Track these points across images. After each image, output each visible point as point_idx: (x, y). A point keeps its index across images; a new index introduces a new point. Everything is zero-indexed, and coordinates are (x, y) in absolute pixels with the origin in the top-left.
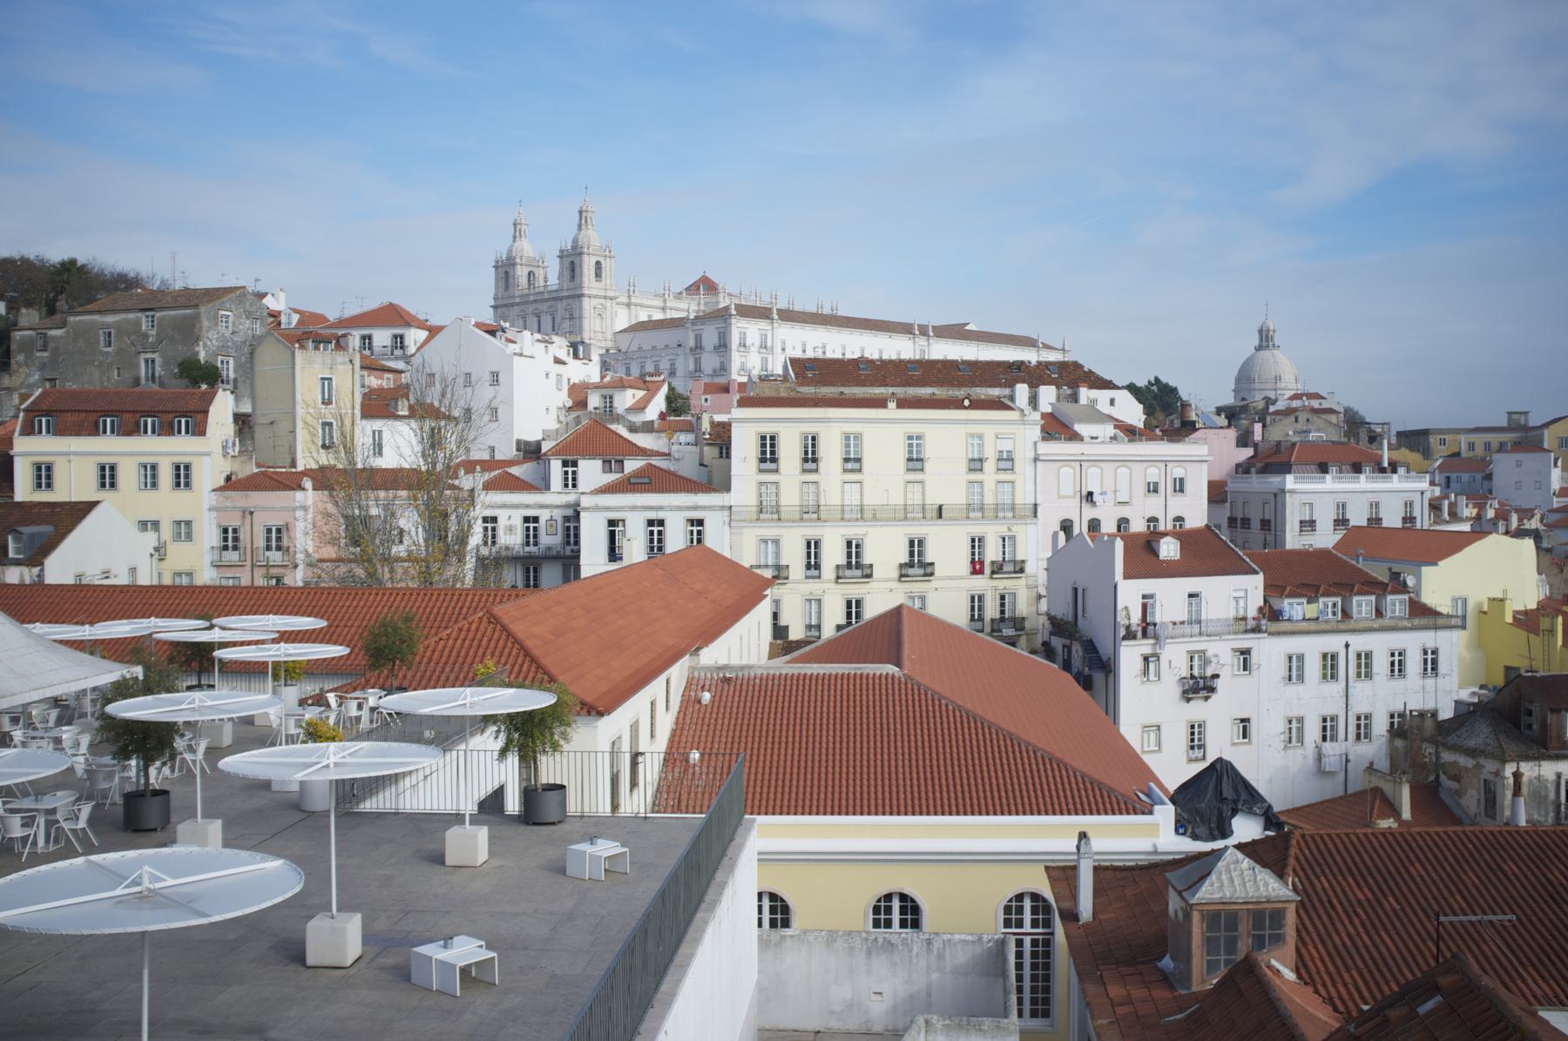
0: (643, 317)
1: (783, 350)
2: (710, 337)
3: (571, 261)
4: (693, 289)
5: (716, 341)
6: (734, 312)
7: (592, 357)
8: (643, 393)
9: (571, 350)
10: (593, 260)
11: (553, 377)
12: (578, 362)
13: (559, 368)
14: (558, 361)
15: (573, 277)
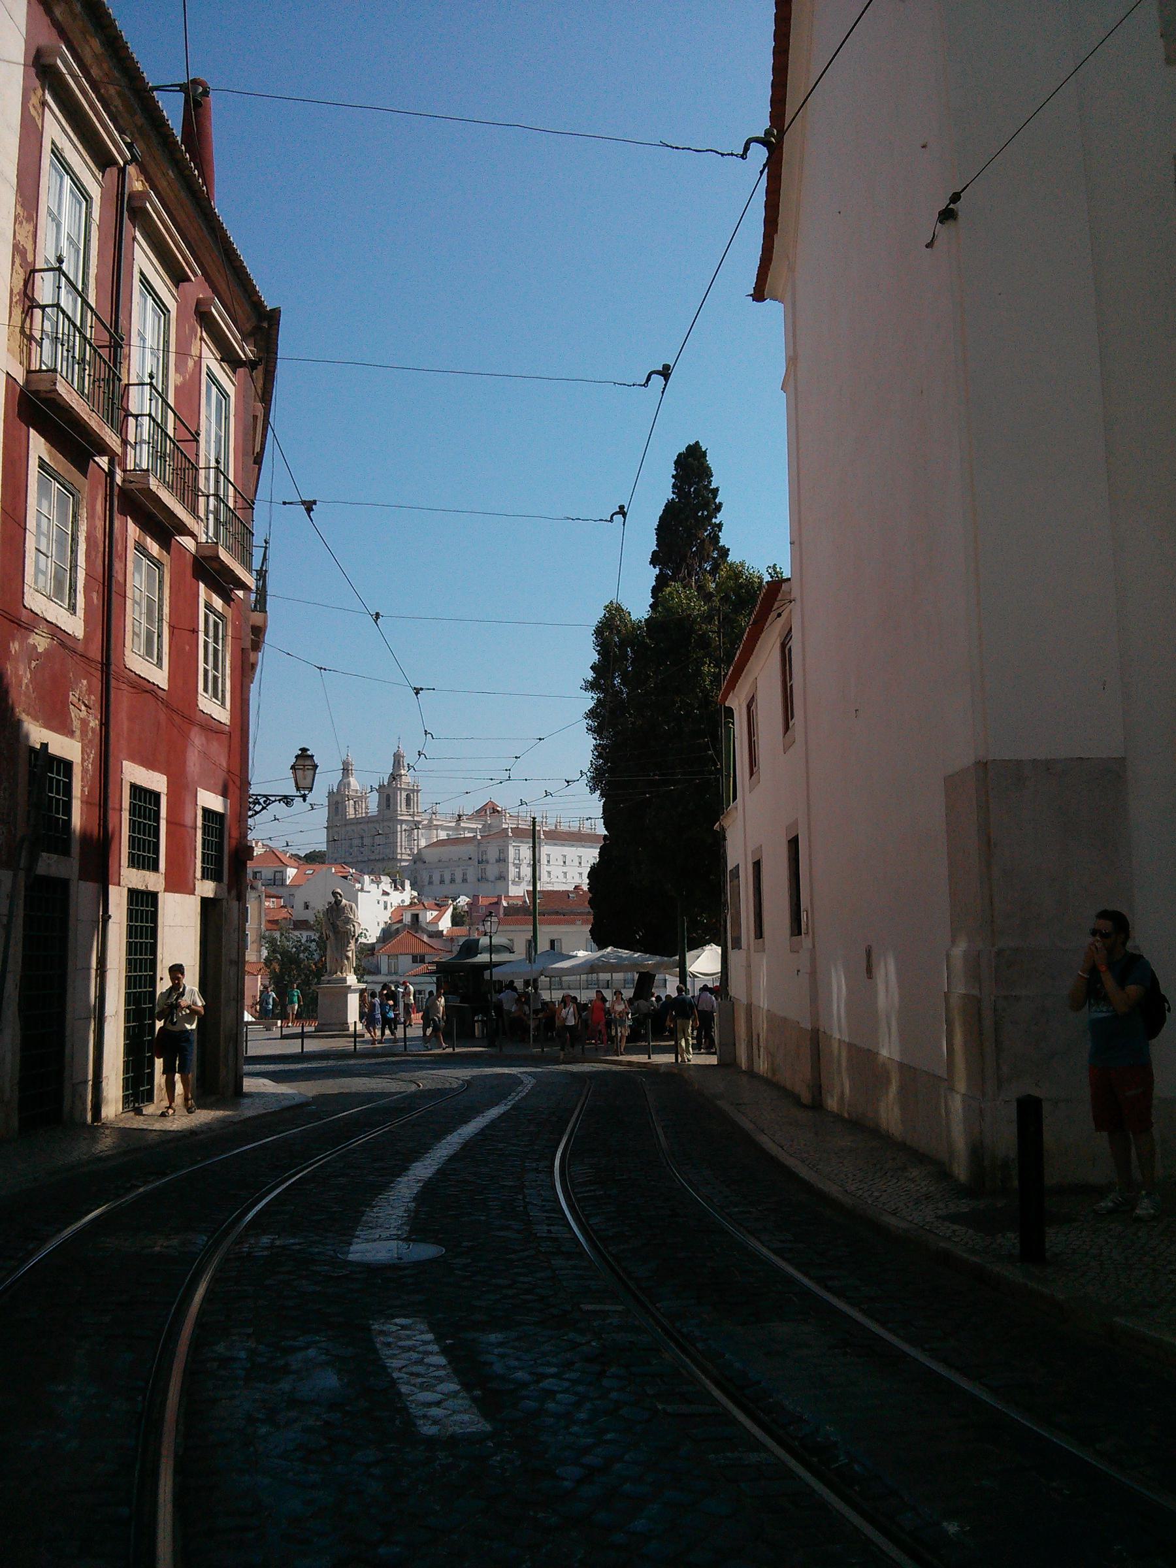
0: (443, 835)
1: (548, 862)
2: (492, 854)
3: (387, 795)
4: (480, 813)
5: (497, 857)
6: (510, 834)
7: (406, 888)
8: (436, 913)
9: (393, 885)
10: (404, 794)
11: (382, 903)
12: (397, 893)
13: (385, 898)
14: (385, 893)
15: (388, 806)
